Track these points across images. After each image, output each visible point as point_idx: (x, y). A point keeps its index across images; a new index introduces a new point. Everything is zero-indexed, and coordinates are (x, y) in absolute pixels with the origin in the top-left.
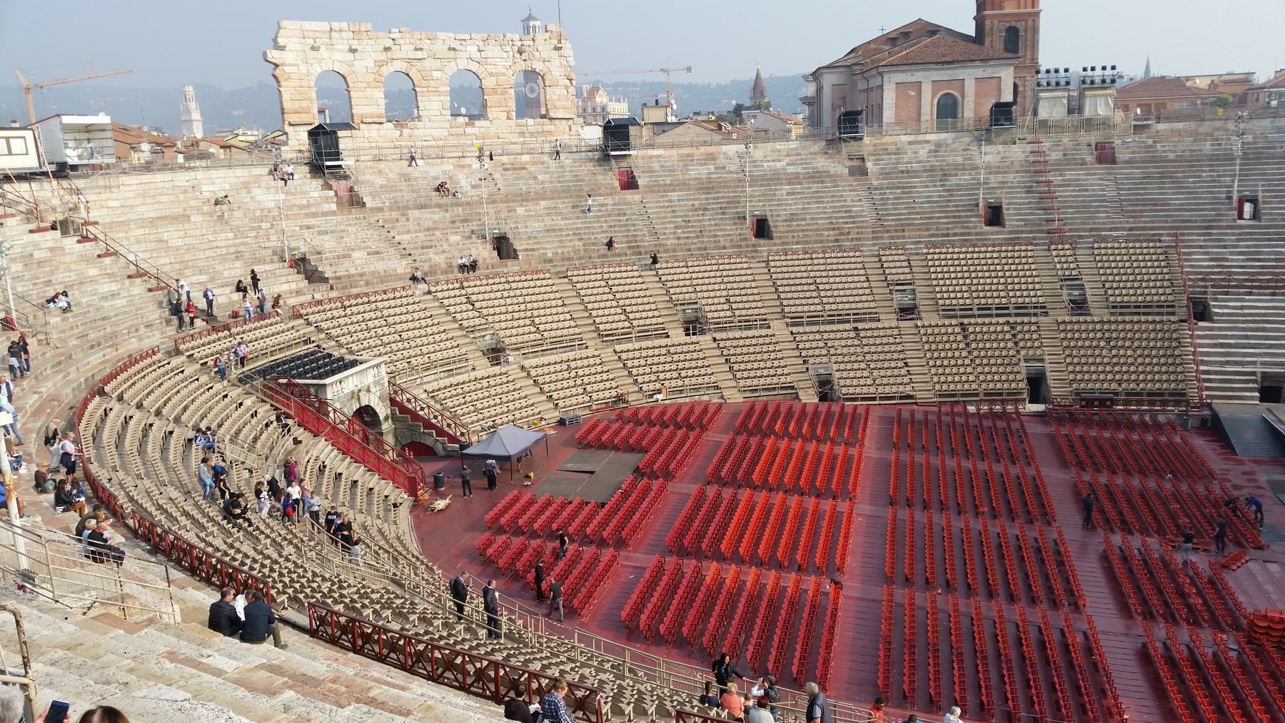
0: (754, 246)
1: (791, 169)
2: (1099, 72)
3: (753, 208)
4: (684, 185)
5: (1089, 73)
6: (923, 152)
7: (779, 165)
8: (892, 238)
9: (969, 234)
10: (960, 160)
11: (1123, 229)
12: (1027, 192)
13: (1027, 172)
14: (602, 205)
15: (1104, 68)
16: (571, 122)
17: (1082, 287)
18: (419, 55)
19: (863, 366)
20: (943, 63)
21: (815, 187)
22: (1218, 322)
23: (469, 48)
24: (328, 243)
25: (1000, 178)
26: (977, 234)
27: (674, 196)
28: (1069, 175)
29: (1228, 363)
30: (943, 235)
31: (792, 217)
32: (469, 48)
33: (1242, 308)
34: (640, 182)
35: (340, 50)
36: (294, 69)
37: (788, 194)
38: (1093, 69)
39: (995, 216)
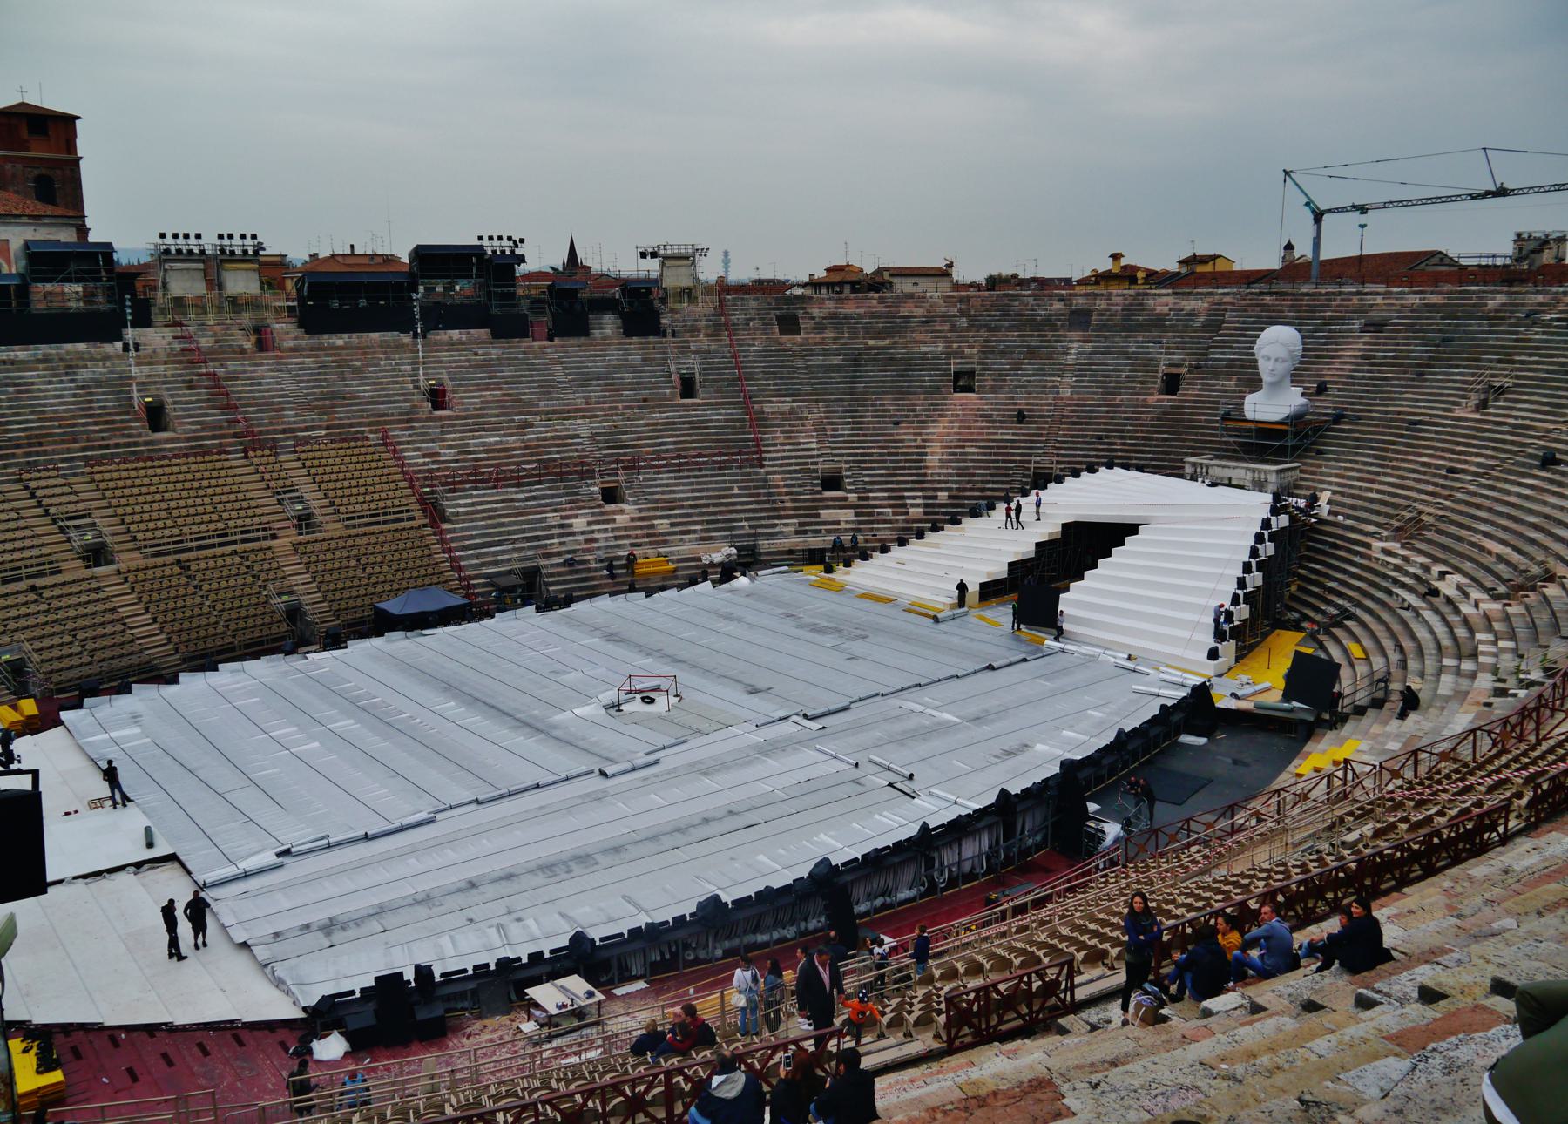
2: (237, 241)
5: (226, 241)
8: (29, 454)
9: (136, 444)
11: (320, 428)
12: (190, 388)
13: (174, 362)
17: (300, 500)
19: (67, 639)
22: (458, 522)
26: (146, 443)
28: (233, 366)
29: (483, 565)
30: (101, 447)
33: (473, 504)
39: (156, 416)
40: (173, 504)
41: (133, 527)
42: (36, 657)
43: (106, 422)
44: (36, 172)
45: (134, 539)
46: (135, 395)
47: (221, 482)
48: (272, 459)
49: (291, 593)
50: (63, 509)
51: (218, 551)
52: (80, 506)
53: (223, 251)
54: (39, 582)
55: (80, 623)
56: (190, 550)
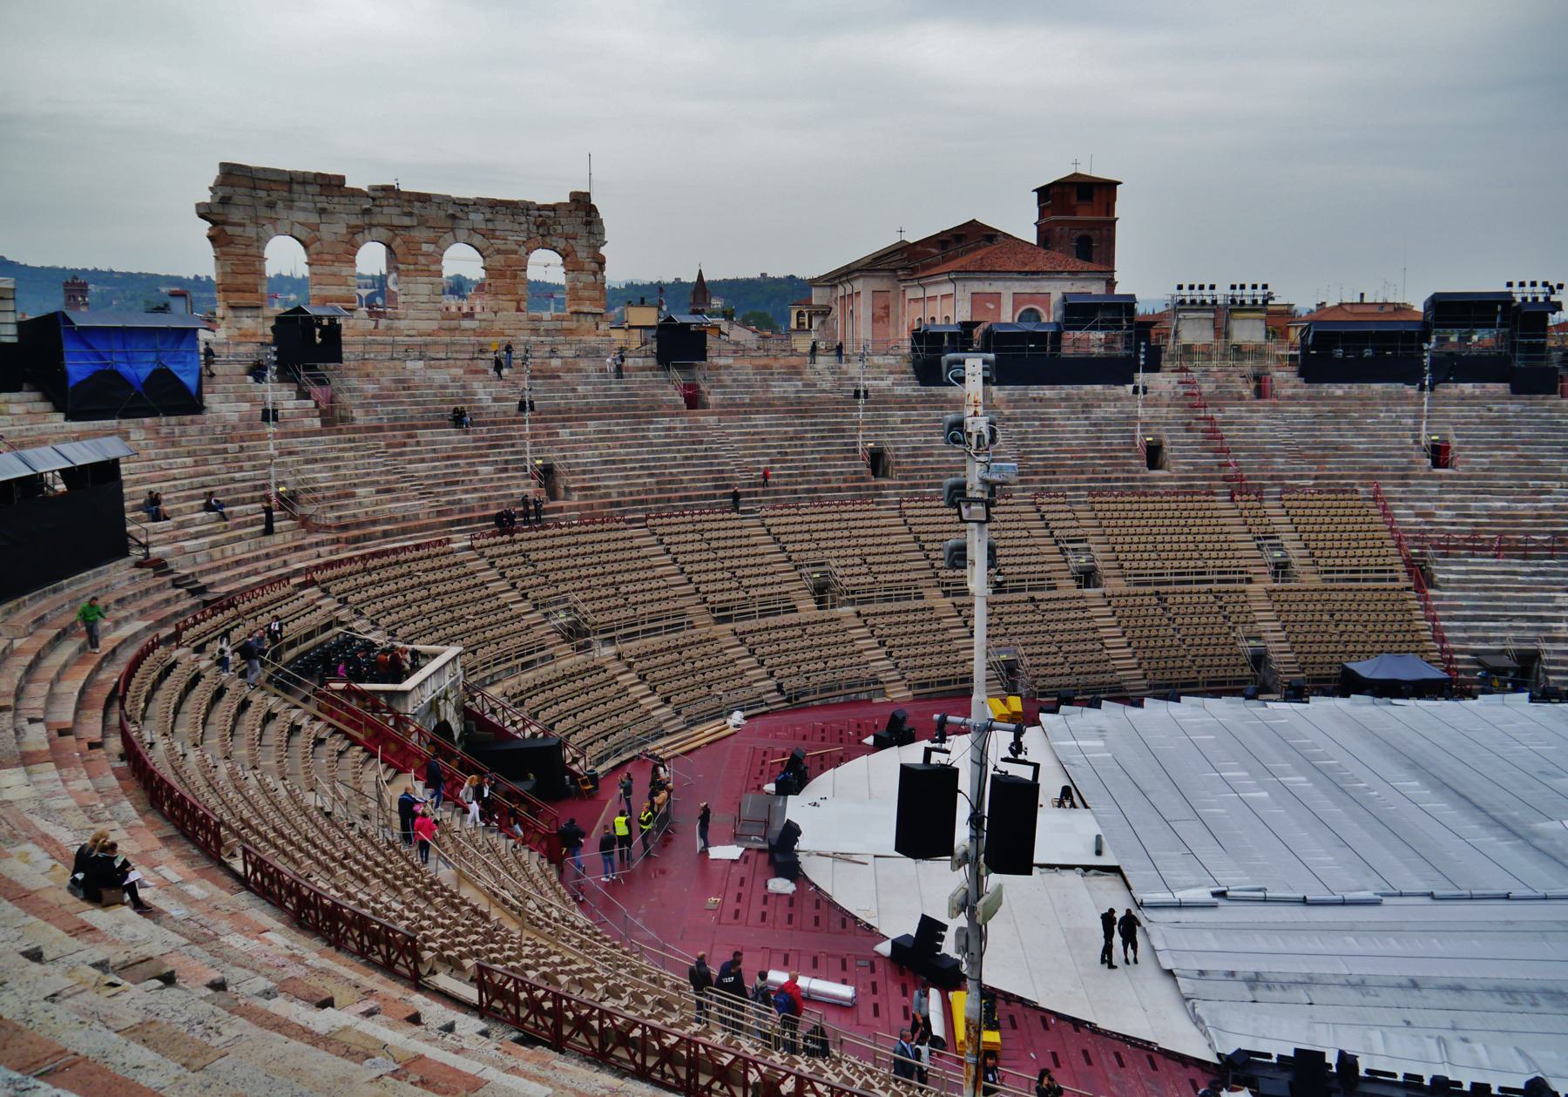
1: (899, 390)
2: (1248, 291)
3: (864, 443)
4: (767, 406)
5: (1238, 292)
8: (1044, 481)
9: (1133, 479)
11: (1309, 477)
12: (1188, 431)
15: (1254, 287)
16: (598, 318)
17: (1280, 547)
18: (407, 221)
19: (1054, 649)
20: (1027, 273)
22: (1446, 589)
23: (472, 216)
24: (321, 476)
26: (1143, 479)
27: (759, 420)
28: (1230, 411)
29: (1471, 639)
30: (1104, 480)
31: (915, 452)
32: (472, 216)
33: (1467, 572)
34: (712, 399)
35: (304, 210)
36: (238, 231)
37: (903, 422)
38: (1243, 287)
39: (1154, 455)
40: (1159, 538)
41: (1122, 556)
42: (1027, 661)
43: (1111, 458)
45: (1121, 567)
46: (1139, 434)
47: (1206, 522)
48: (1257, 504)
49: (1258, 638)
50: (1066, 532)
51: (1195, 587)
52: (1080, 532)
53: (1233, 302)
54: (1038, 595)
55: (1066, 637)
56: (1169, 583)
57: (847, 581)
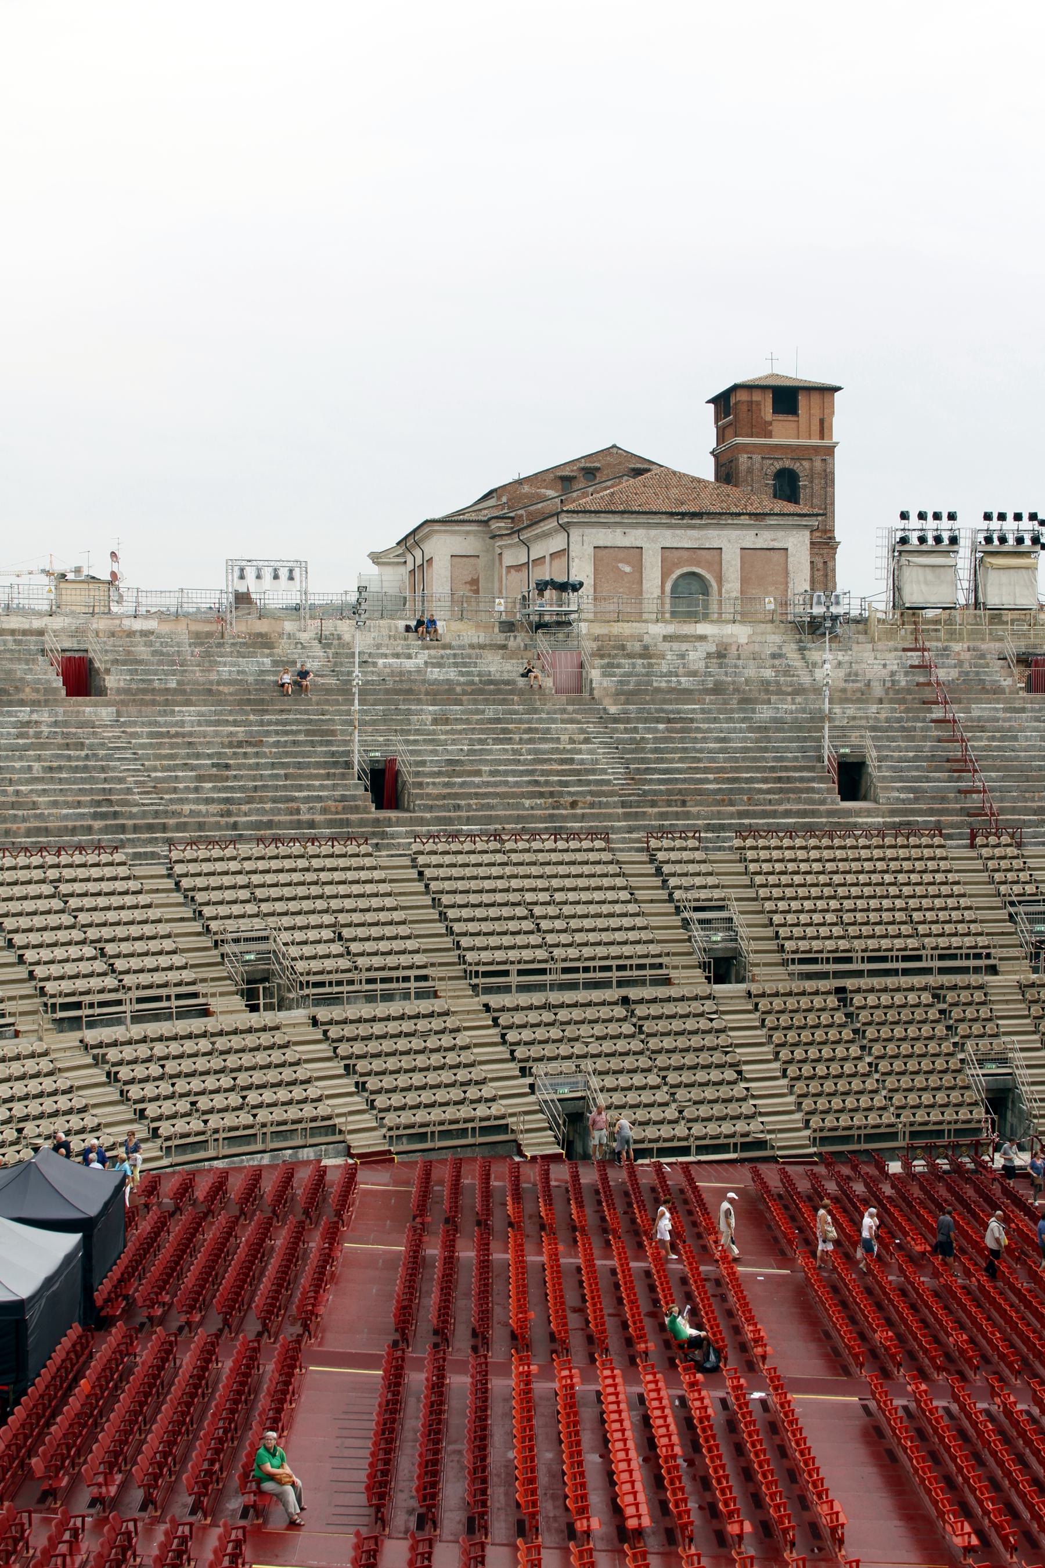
0: (377, 822)
1: (435, 674)
3: (362, 748)
4: (209, 693)
6: (696, 657)
7: (409, 664)
8: (663, 816)
9: (814, 813)
10: (768, 674)
14: (28, 724)
19: (653, 1079)
21: (491, 711)
25: (851, 710)
26: (830, 813)
27: (188, 715)
28: (978, 710)
34: (110, 682)
37: (435, 722)
39: (851, 779)
40: (848, 904)
41: (783, 932)
42: (602, 1100)
43: (779, 780)
44: (778, 465)
45: (782, 949)
46: (826, 743)
47: (927, 878)
48: (1011, 851)
49: (1003, 1061)
50: (691, 895)
51: (905, 981)
52: (717, 894)
53: (989, 540)
54: (633, 993)
55: (676, 1060)
56: (859, 974)
57: (301, 966)
